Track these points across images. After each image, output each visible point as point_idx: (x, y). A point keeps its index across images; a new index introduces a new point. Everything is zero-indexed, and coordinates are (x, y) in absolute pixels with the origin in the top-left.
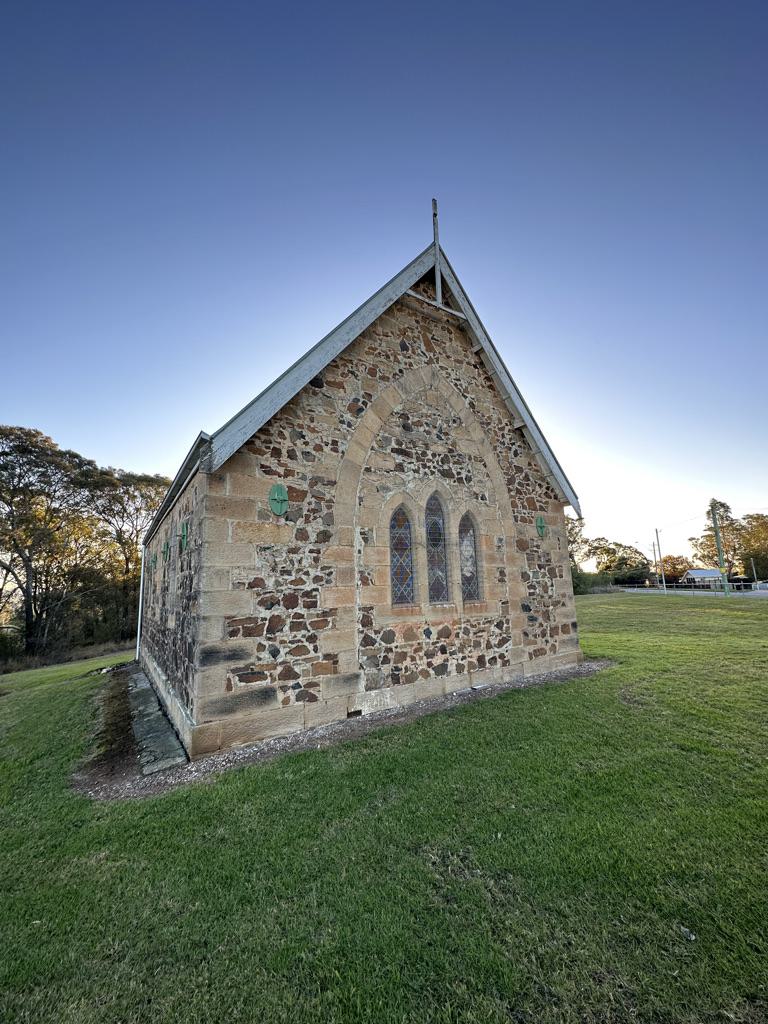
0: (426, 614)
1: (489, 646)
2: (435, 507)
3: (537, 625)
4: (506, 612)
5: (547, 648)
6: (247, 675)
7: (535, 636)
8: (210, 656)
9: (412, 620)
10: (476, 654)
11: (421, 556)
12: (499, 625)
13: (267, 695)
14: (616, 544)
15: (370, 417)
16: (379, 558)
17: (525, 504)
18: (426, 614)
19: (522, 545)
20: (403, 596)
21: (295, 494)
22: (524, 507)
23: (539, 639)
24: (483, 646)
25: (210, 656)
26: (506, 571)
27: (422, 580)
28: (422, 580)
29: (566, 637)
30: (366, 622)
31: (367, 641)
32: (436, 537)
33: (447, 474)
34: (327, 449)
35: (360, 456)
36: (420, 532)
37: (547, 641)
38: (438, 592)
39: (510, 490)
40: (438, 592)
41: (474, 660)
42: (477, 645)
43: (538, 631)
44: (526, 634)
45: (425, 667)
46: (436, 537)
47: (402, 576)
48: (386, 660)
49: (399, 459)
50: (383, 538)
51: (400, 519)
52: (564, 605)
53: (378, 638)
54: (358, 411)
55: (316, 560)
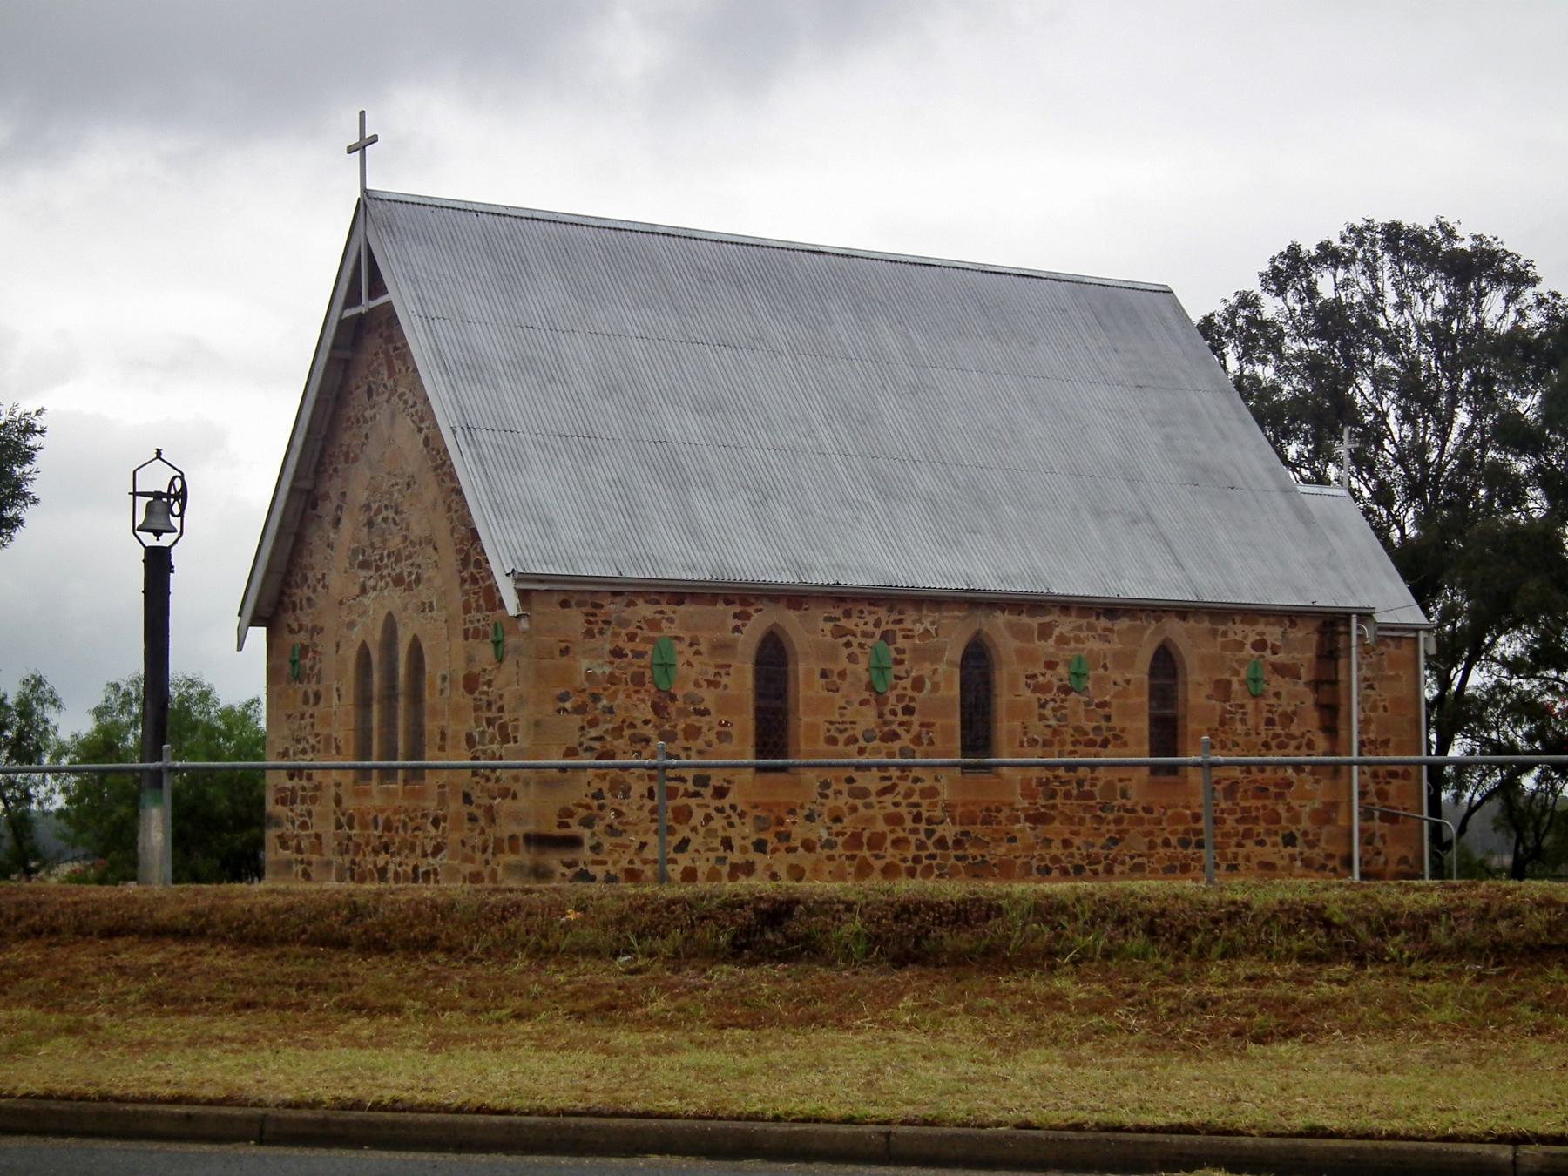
1: (425, 855)
3: (478, 831)
4: (442, 800)
5: (486, 872)
7: (473, 848)
9: (367, 804)
10: (412, 862)
12: (436, 823)
17: (482, 602)
19: (471, 683)
22: (479, 609)
23: (478, 856)
24: (419, 851)
26: (449, 733)
29: (512, 858)
30: (338, 801)
31: (339, 826)
34: (319, 587)
37: (487, 862)
39: (463, 581)
41: (409, 869)
42: (413, 848)
43: (477, 841)
44: (463, 843)
45: (370, 866)
48: (347, 851)
49: (362, 573)
52: (515, 797)
53: (343, 820)
55: (312, 725)
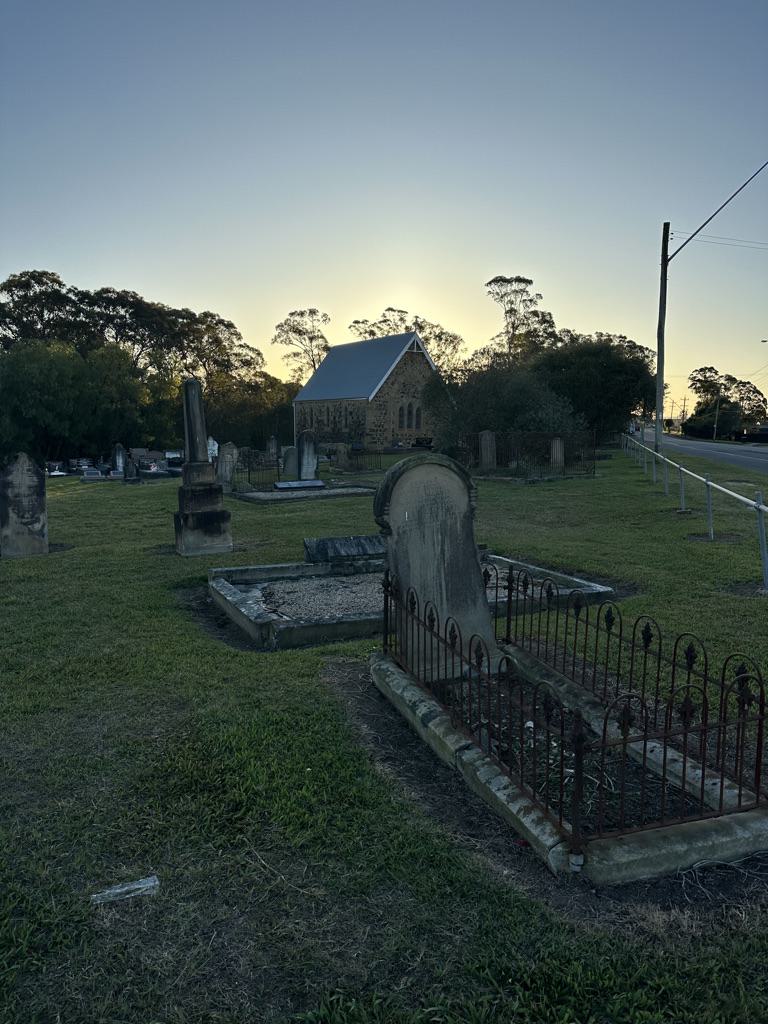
0: (406, 431)
2: (410, 405)
6: (374, 438)
8: (367, 435)
11: (406, 418)
13: (375, 442)
14: (731, 379)
15: (396, 386)
16: (396, 419)
18: (406, 431)
20: (401, 427)
21: (381, 405)
25: (367, 435)
27: (406, 424)
28: (406, 424)
32: (410, 413)
33: (414, 397)
35: (393, 395)
36: (406, 412)
38: (409, 426)
40: (409, 426)
46: (410, 413)
47: (401, 422)
50: (397, 413)
51: (401, 409)
54: (393, 384)
